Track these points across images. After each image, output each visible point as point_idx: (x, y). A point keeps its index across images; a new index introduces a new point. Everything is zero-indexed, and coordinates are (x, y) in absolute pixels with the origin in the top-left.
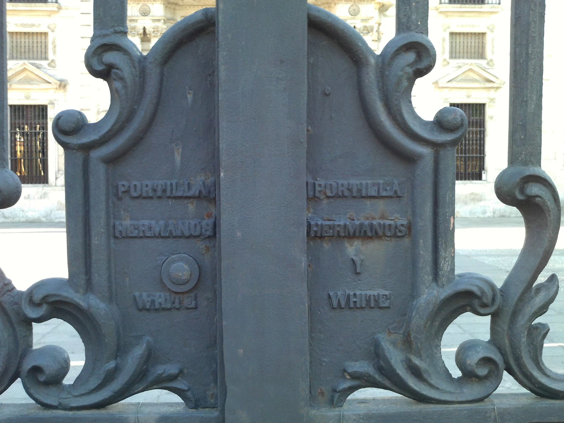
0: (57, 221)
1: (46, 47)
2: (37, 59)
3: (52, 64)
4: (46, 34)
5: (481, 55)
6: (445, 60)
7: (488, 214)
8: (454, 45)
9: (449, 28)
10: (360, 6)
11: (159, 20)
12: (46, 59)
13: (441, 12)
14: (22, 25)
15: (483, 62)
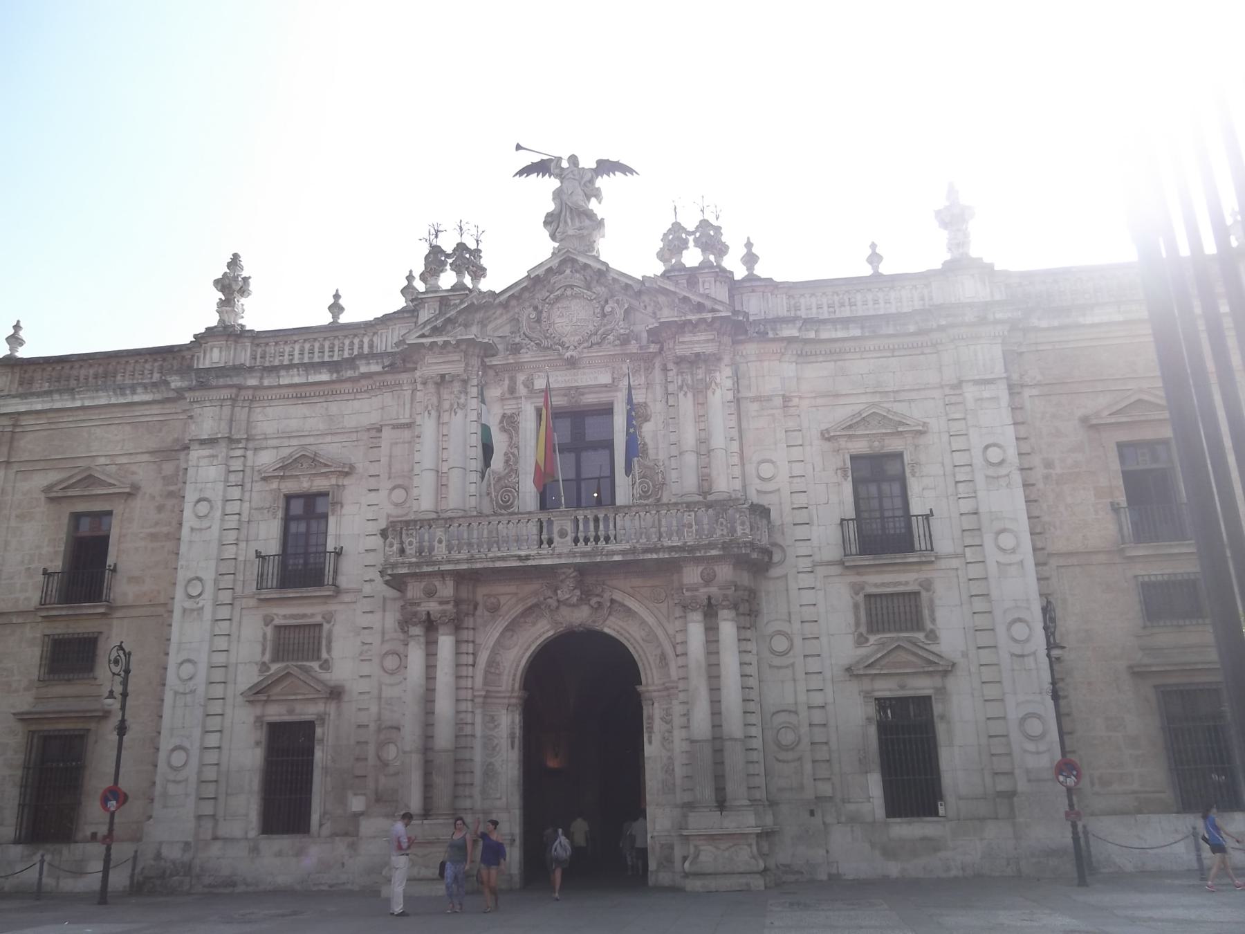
0: (315, 889)
1: (320, 643)
2: (308, 660)
3: (326, 666)
4: (321, 625)
5: (918, 625)
6: (861, 635)
7: (953, 873)
8: (874, 612)
9: (863, 588)
10: (716, 568)
11: (448, 602)
12: (319, 658)
13: (847, 567)
14: (293, 616)
15: (920, 636)
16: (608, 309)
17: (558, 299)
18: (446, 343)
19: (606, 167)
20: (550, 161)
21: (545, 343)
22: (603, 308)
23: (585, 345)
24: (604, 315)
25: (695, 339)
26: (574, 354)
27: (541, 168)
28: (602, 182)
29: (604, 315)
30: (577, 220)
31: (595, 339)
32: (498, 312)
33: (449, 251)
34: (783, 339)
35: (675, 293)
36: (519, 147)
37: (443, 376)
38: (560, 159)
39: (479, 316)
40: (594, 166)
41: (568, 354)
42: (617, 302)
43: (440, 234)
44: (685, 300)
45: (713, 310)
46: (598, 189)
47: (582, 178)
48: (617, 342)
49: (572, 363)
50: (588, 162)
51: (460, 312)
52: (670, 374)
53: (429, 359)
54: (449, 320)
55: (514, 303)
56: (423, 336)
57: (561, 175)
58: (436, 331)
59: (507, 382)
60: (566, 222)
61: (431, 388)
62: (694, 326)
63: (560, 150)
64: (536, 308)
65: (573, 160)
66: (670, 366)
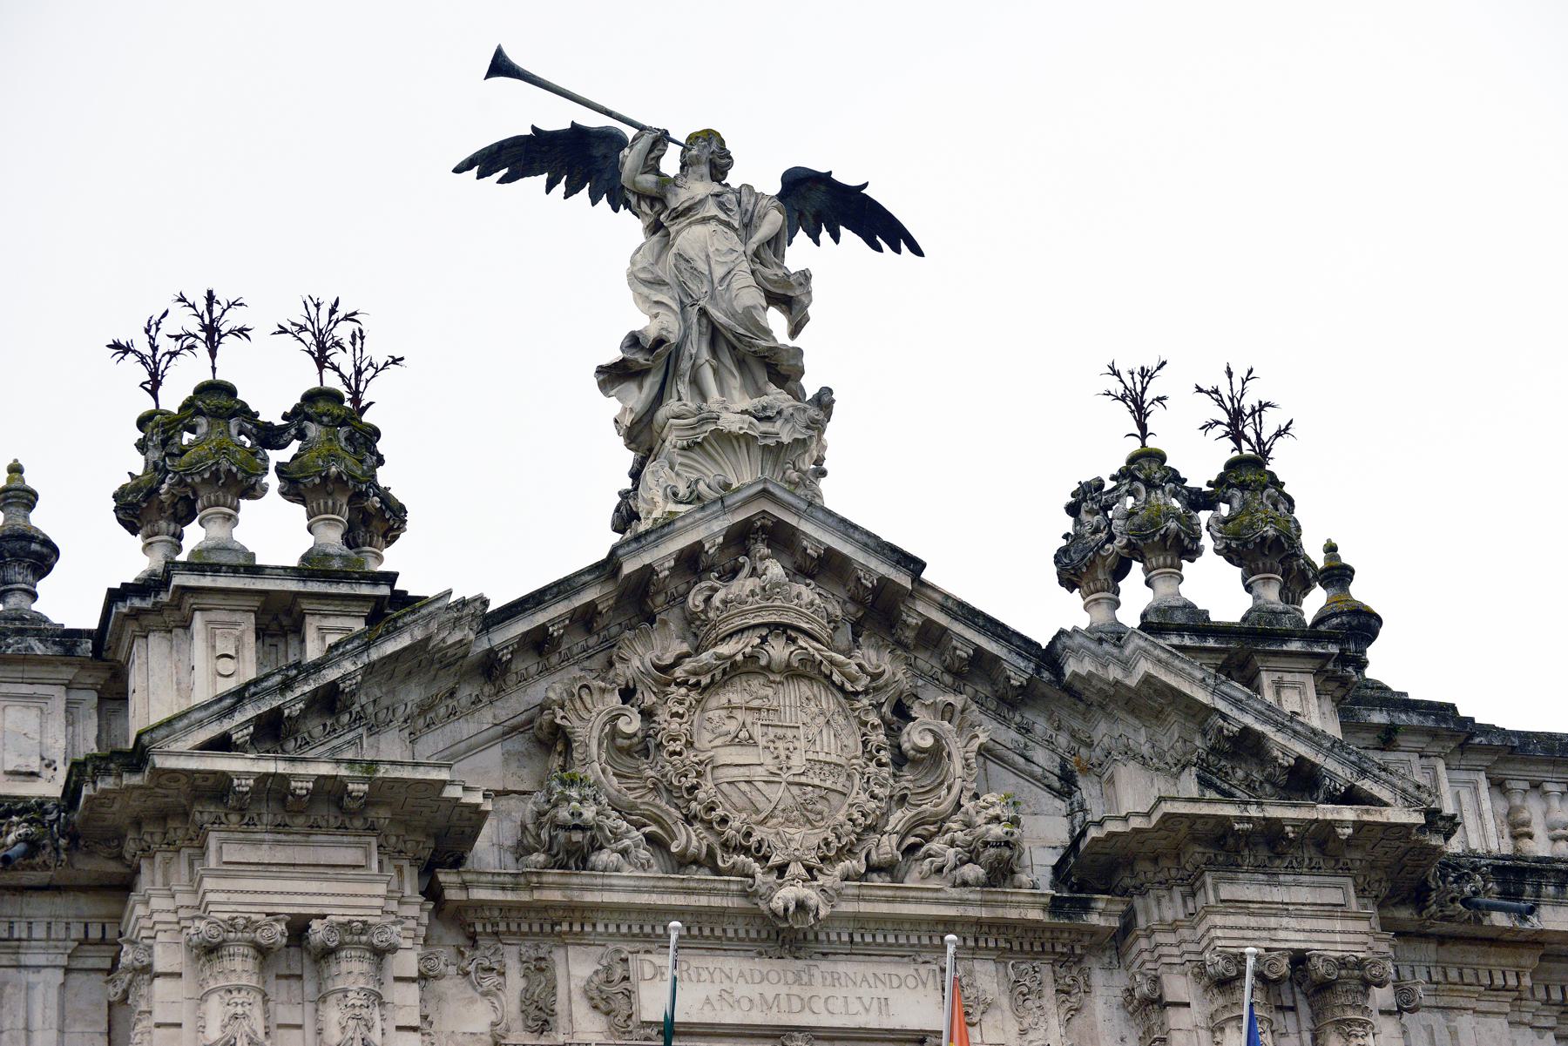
16: (916, 737)
17: (733, 670)
18: (329, 792)
19: (823, 202)
20: (612, 140)
21: (689, 839)
22: (893, 731)
23: (848, 864)
24: (901, 759)
25: (1277, 895)
26: (812, 896)
27: (576, 158)
28: (801, 253)
29: (901, 759)
30: (735, 382)
31: (886, 847)
32: (466, 693)
33: (272, 411)
34: (1539, 942)
35: (1199, 714)
36: (500, 66)
37: (298, 928)
38: (662, 139)
39: (414, 694)
40: (775, 187)
41: (786, 895)
42: (947, 712)
43: (228, 345)
44: (1248, 745)
45: (1351, 797)
46: (805, 276)
47: (748, 226)
48: (972, 871)
49: (786, 937)
50: (758, 172)
51: (370, 668)
52: (1175, 1018)
53: (223, 848)
54: (329, 701)
55: (527, 664)
56: (222, 744)
57: (658, 208)
58: (272, 731)
59: (515, 982)
60: (696, 383)
61: (240, 968)
62: (1228, 847)
63: (651, 95)
64: (627, 694)
65: (710, 154)
66: (1178, 986)
